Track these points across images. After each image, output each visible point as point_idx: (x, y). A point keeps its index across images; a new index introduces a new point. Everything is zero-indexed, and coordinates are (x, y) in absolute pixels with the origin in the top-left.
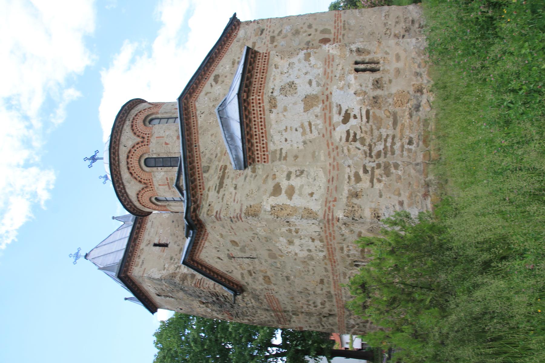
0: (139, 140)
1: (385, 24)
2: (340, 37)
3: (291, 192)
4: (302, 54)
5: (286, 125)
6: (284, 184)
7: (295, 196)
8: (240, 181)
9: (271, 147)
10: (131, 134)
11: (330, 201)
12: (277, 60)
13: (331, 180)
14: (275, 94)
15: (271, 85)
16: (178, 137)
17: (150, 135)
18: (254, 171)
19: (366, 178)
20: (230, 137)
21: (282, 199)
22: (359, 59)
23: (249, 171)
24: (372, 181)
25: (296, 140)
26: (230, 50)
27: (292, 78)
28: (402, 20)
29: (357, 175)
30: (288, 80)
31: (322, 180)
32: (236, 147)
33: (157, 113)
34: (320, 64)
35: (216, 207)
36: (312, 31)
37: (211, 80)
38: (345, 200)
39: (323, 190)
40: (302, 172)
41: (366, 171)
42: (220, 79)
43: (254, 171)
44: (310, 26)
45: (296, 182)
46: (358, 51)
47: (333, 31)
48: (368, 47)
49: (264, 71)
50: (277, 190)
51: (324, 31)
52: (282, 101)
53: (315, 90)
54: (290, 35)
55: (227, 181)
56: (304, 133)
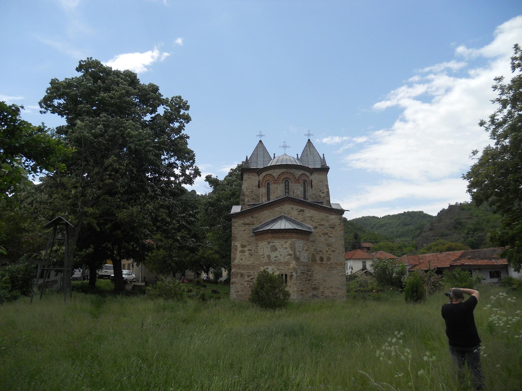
0: (276, 178)
1: (332, 287)
2: (324, 266)
3: (243, 252)
4: (292, 253)
5: (264, 247)
6: (246, 249)
7: (241, 253)
8: (247, 232)
9: (259, 242)
10: (279, 173)
11: (239, 266)
12: (290, 242)
13: (248, 266)
14: (271, 244)
15: (276, 241)
16: (277, 197)
17: (278, 183)
18: (252, 236)
19: (249, 279)
20: (268, 224)
21: (239, 249)
22: (288, 276)
23: (252, 234)
24: (248, 281)
25: (261, 252)
26: (320, 213)
27: (279, 250)
28: (334, 295)
29: (250, 276)
30: (278, 248)
31: (248, 263)
32: (262, 228)
33: (291, 183)
34: (286, 260)
35: (236, 225)
36: (330, 252)
37: (301, 208)
38: (240, 272)
39: (243, 263)
40: (251, 255)
41: (252, 279)
42: (301, 213)
43: (252, 236)
44: (333, 251)
45: (247, 253)
46: (292, 275)
47: (329, 263)
48: (293, 279)
49: (283, 238)
50: (243, 246)
51: (329, 259)
52: (269, 246)
53: (273, 259)
54: (328, 242)
55: (247, 226)
56: (262, 255)
